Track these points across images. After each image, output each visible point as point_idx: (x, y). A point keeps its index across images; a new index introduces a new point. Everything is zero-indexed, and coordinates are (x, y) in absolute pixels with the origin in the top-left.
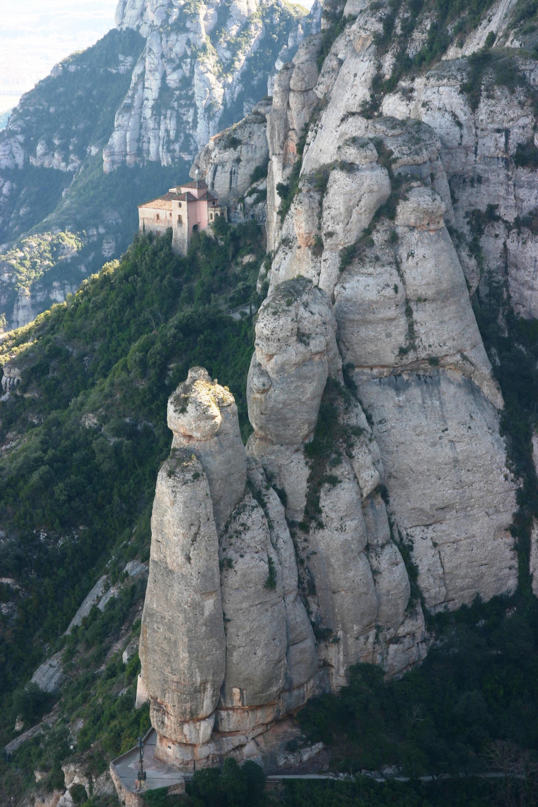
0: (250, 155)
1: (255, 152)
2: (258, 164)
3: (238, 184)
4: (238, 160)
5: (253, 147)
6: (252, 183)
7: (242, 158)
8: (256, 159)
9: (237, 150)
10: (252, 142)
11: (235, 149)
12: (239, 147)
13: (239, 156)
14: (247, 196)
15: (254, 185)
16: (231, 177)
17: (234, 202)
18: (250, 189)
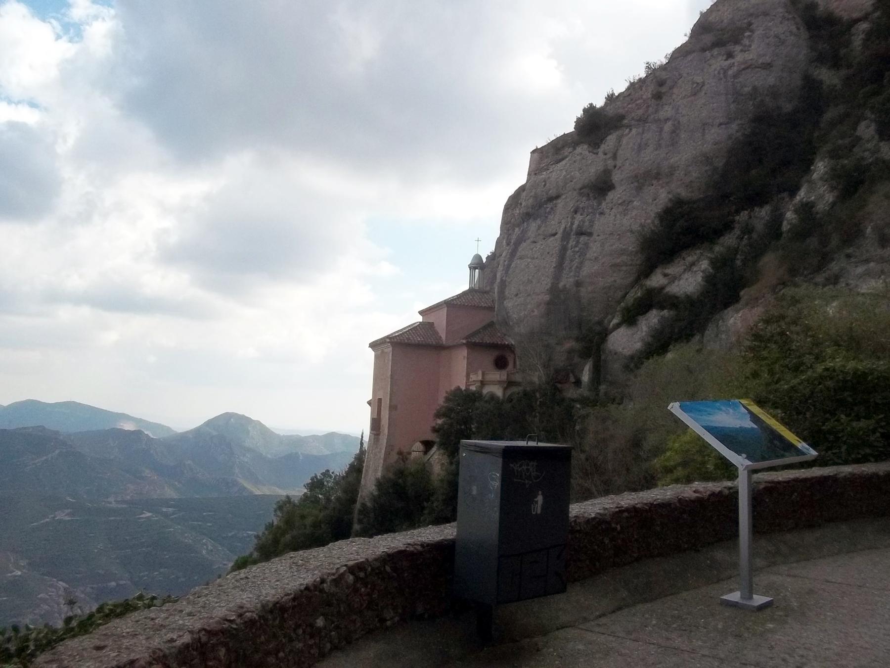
0: (649, 156)
1: (674, 143)
2: (684, 193)
3: (586, 270)
4: (601, 187)
5: (668, 127)
6: (647, 271)
7: (616, 177)
8: (673, 169)
9: (603, 147)
10: (667, 111)
11: (595, 145)
12: (611, 139)
13: (607, 173)
14: (618, 326)
15: (656, 280)
16: (564, 249)
17: (570, 352)
18: (636, 293)
